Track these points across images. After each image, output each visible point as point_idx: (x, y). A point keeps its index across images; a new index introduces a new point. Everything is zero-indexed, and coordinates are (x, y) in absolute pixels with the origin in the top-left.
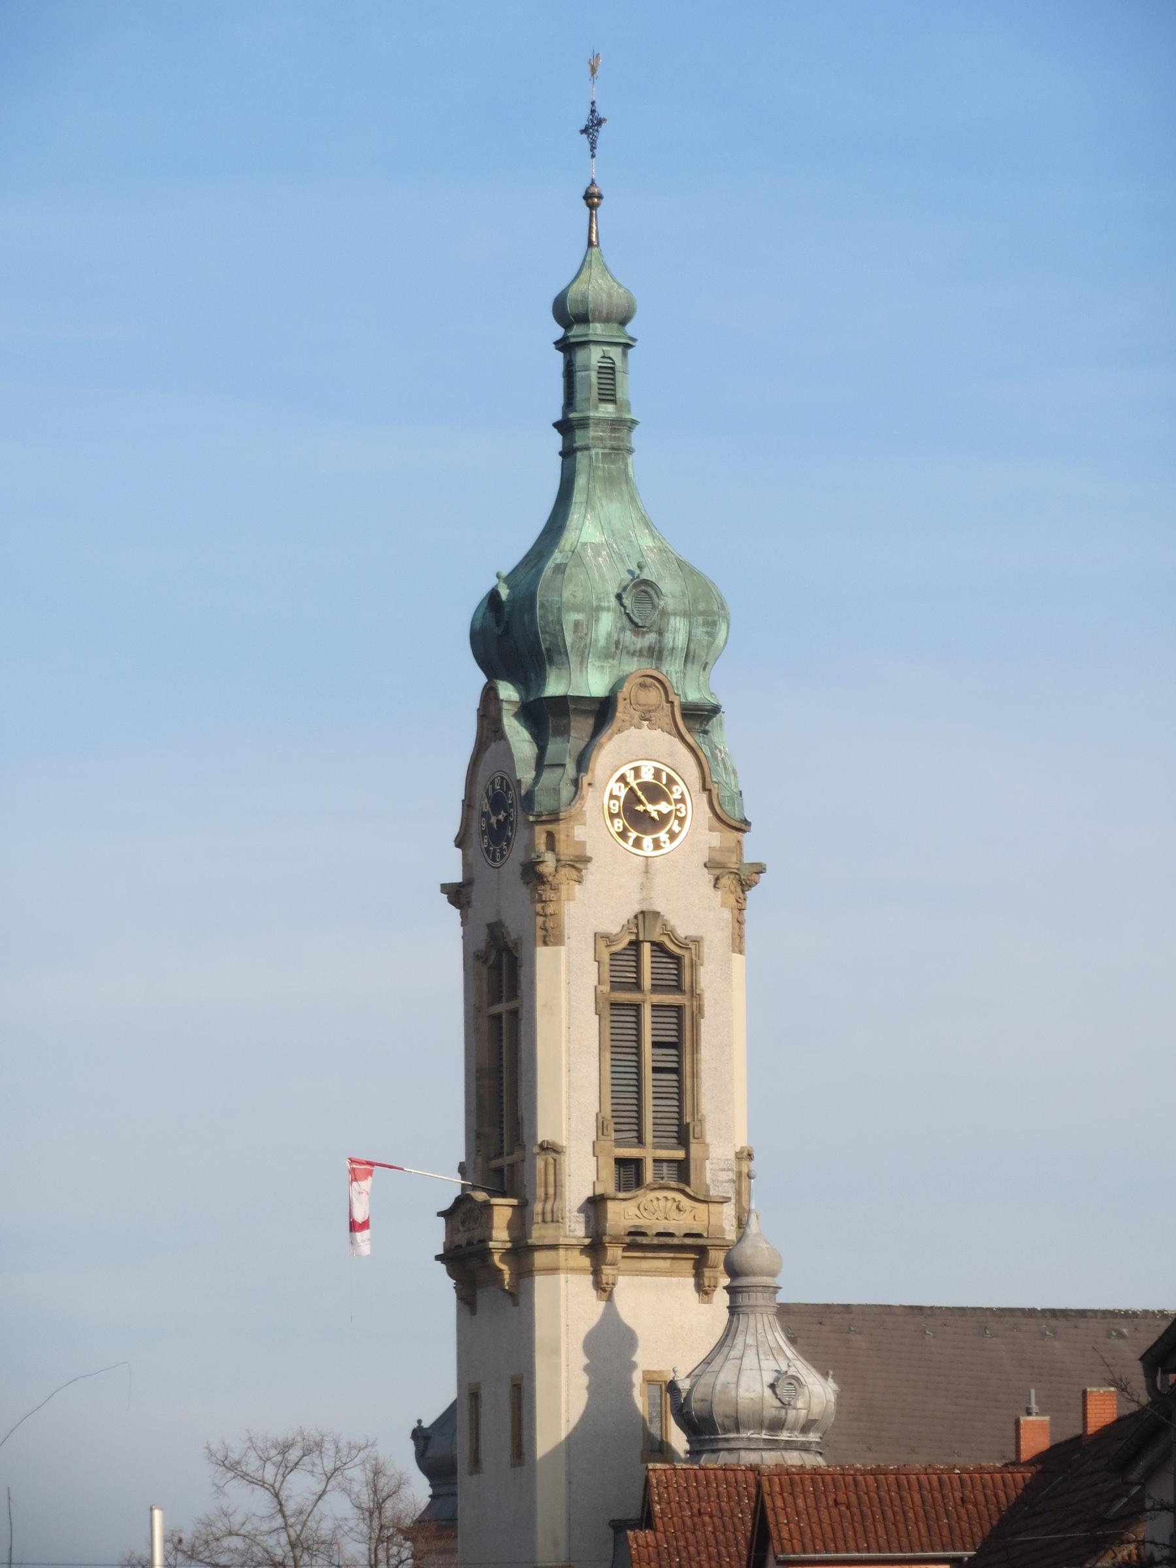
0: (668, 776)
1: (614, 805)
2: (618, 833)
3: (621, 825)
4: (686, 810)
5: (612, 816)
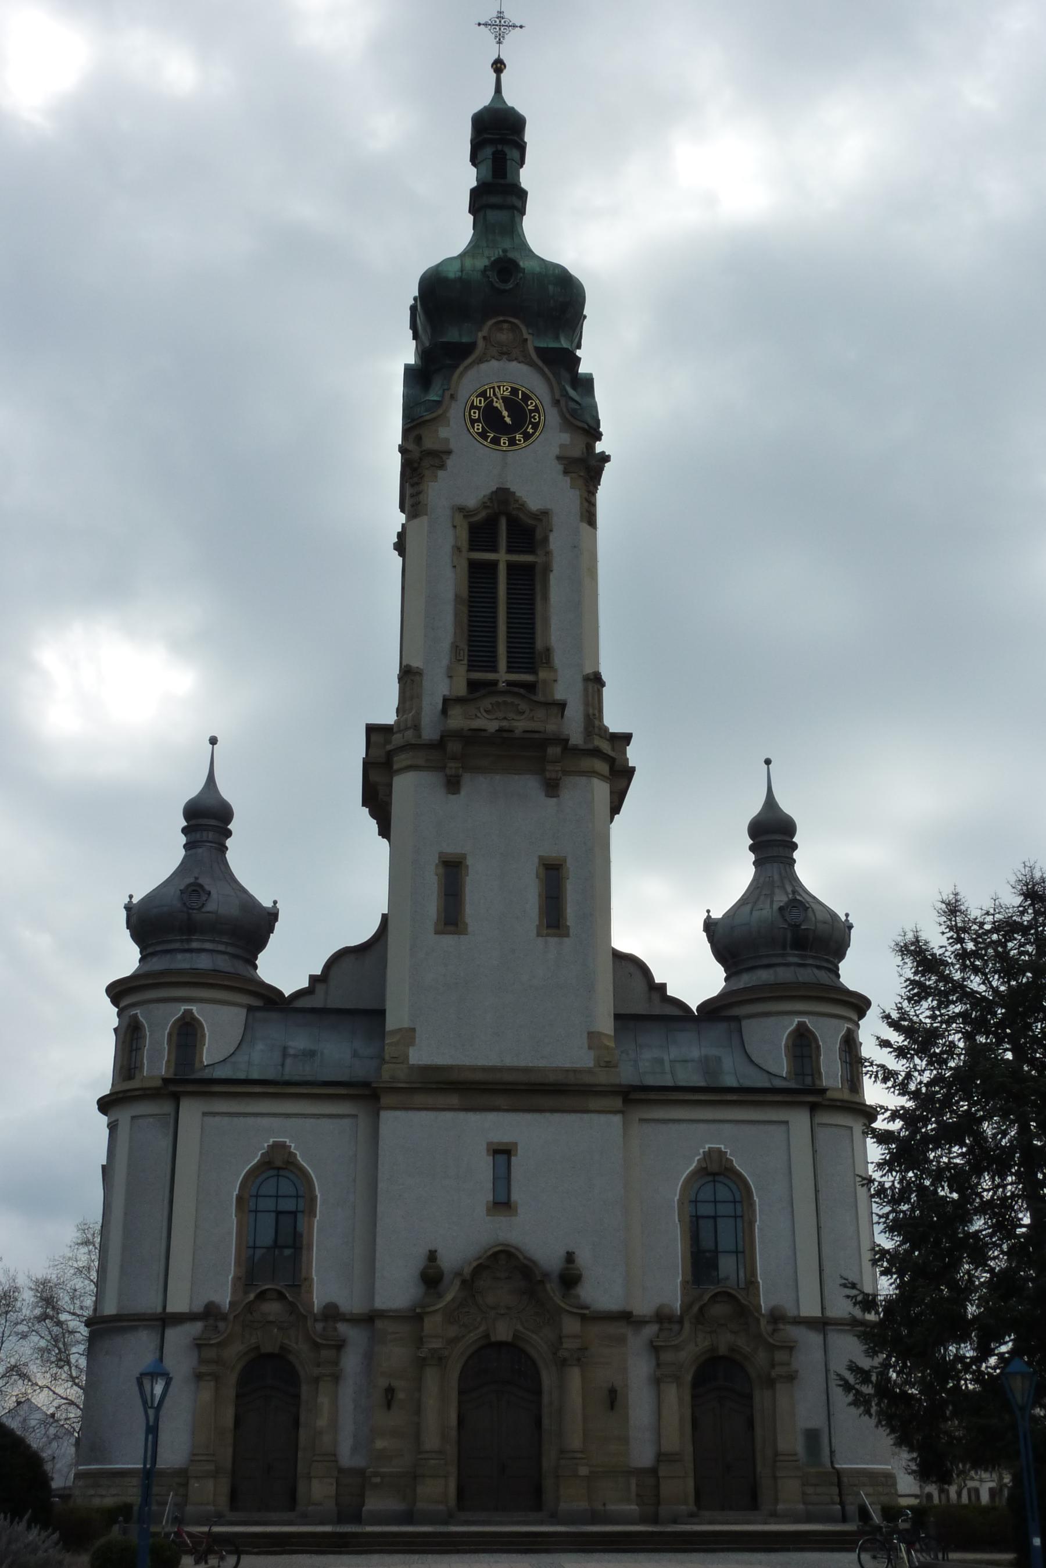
0: (522, 391)
1: (475, 413)
2: (477, 433)
3: (480, 427)
4: (539, 417)
5: (473, 422)
